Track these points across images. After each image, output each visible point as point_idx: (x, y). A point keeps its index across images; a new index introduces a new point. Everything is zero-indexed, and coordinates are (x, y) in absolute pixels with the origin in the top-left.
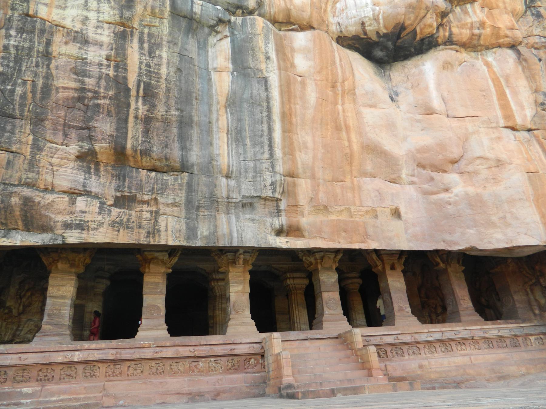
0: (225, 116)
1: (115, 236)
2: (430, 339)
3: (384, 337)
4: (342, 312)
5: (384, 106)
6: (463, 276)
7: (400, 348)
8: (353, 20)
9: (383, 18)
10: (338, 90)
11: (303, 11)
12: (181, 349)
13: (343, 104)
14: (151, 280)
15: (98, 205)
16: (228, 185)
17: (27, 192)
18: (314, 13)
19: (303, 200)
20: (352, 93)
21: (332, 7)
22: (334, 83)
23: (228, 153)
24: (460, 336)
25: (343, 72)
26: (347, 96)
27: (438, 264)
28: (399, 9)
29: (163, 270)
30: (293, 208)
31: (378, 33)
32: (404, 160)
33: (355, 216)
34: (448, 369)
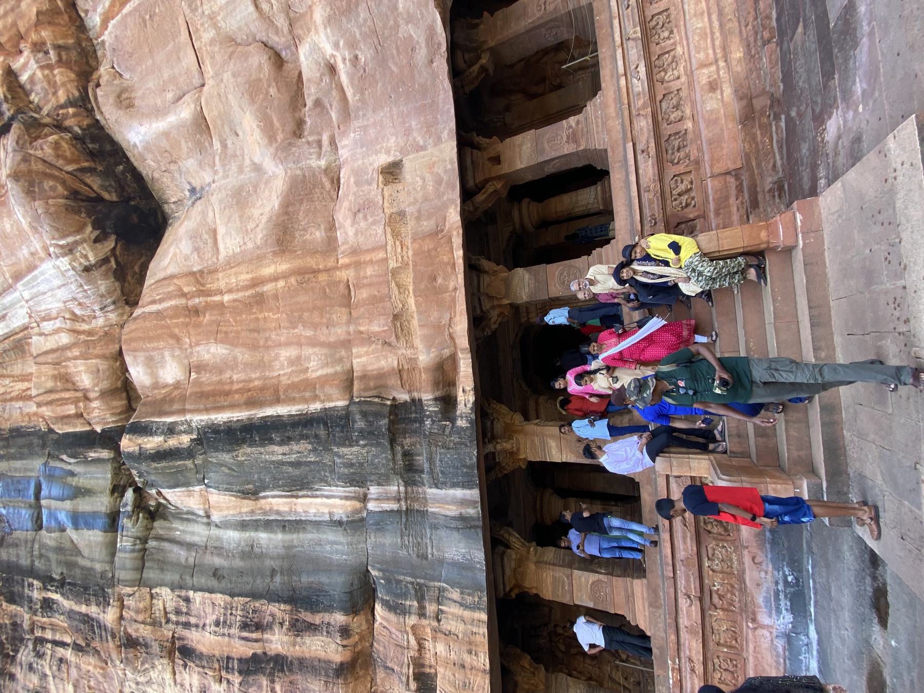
0: (270, 500)
2: (642, 69)
3: (644, 182)
4: (585, 258)
5: (211, 214)
7: (667, 140)
8: (86, 288)
9: (63, 237)
10: (200, 302)
11: (98, 371)
12: (684, 621)
13: (221, 293)
14: (550, 589)
16: (376, 499)
18: (96, 352)
20: (201, 276)
21: (84, 321)
22: (189, 311)
23: (328, 497)
25: (169, 297)
27: (483, 69)
28: (40, 211)
29: (532, 567)
30: (405, 377)
31: (96, 241)
32: (291, 165)
33: (405, 258)
34: (714, 17)
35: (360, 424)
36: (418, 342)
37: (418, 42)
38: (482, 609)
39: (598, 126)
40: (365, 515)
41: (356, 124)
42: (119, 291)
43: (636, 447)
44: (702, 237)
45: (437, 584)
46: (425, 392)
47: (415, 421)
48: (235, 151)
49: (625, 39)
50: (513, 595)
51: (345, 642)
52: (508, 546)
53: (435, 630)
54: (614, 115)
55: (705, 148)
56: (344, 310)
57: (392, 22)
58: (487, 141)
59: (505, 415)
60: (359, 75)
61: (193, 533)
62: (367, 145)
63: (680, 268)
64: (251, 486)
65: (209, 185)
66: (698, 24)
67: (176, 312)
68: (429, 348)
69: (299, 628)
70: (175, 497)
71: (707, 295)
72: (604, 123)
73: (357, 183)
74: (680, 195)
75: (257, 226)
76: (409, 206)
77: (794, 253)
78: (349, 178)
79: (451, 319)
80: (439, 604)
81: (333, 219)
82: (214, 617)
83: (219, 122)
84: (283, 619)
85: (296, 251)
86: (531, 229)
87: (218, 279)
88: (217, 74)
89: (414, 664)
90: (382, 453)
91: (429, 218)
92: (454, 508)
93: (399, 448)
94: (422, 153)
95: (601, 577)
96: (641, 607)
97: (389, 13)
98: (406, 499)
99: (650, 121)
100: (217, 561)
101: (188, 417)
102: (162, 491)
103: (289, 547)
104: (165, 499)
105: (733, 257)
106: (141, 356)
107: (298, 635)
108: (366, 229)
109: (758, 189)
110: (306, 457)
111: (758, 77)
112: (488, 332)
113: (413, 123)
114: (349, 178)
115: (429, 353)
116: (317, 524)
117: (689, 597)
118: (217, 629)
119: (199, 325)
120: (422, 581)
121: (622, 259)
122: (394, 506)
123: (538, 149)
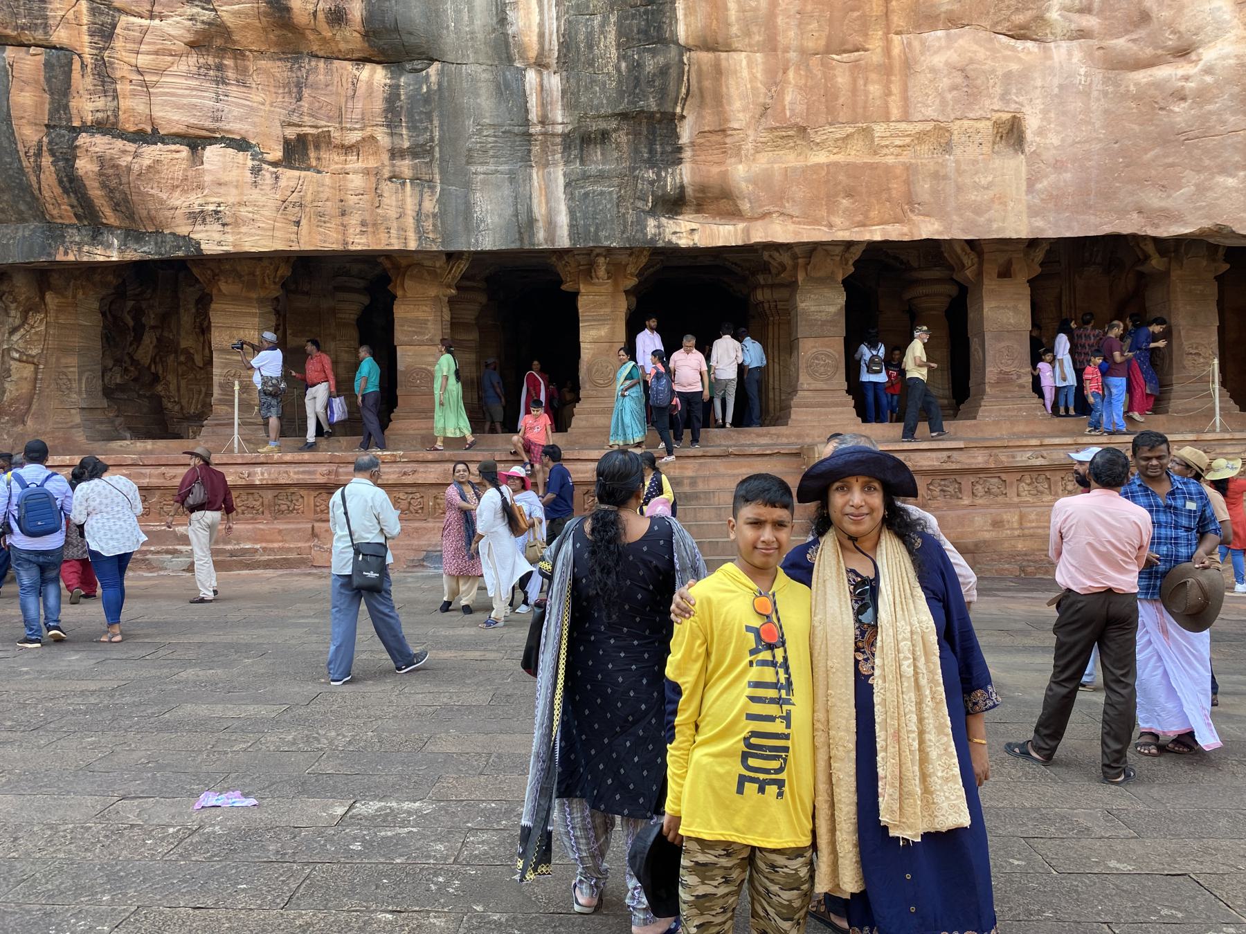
1: (293, 237)
3: (917, 454)
14: (409, 315)
15: (250, 163)
16: (542, 86)
17: (99, 143)
19: (739, 113)
27: (1147, 257)
29: (433, 292)
30: (714, 138)
33: (885, 151)
35: (651, 65)
37: (1169, 196)
41: (1098, 76)
45: (437, 177)
46: (692, 169)
47: (651, 151)
51: (321, 16)
54: (1015, 430)
56: (823, 42)
57: (1207, 162)
60: (1159, 99)
68: (754, 181)
73: (1008, 76)
76: (957, 162)
79: (792, 217)
89: (318, 136)
90: (608, 99)
91: (935, 192)
92: (543, 211)
94: (1024, 188)
97: (1219, 161)
98: (544, 134)
108: (936, 89)
113: (1068, 176)
114: (1020, 59)
115: (748, 180)
120: (437, 155)
122: (534, 116)
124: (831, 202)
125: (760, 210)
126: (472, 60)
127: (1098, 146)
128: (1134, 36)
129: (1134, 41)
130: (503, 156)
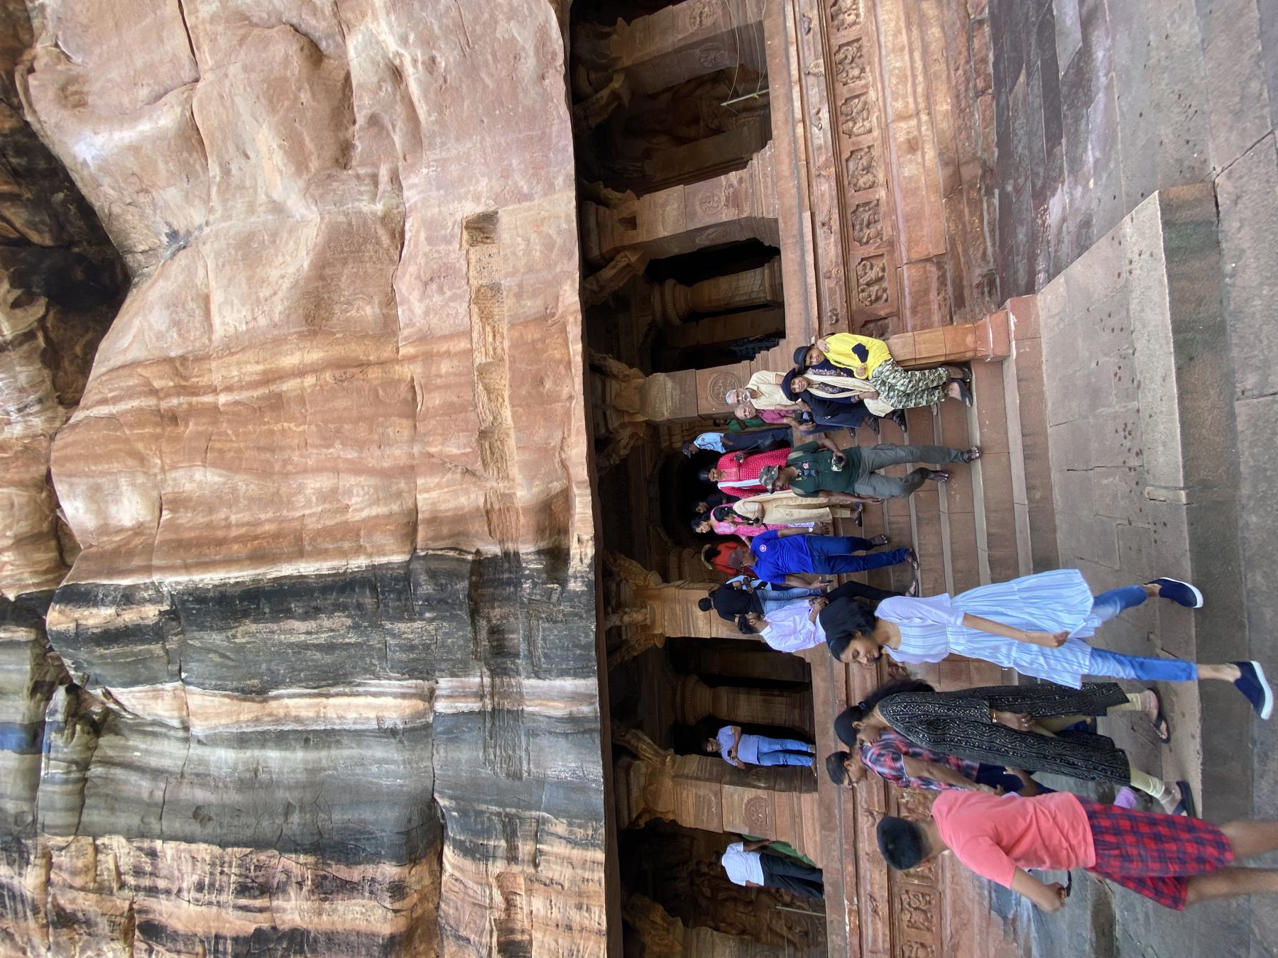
0: (286, 701)
2: (825, 115)
3: (821, 265)
5: (201, 272)
6: (640, 19)
7: (854, 212)
10: (180, 404)
13: (215, 391)
14: (692, 811)
16: (449, 697)
19: (470, 498)
20: (182, 365)
22: (162, 417)
23: (375, 695)
24: (814, 14)
25: (129, 394)
26: (195, 380)
27: (615, 96)
29: (668, 783)
33: (499, 351)
34: (917, 55)
35: (426, 588)
36: (515, 472)
37: (523, 48)
38: (598, 846)
39: (766, 187)
40: (431, 719)
41: (430, 155)
42: (48, 383)
43: (807, 615)
44: (894, 340)
45: (534, 813)
46: (524, 542)
48: (242, 181)
49: (803, 73)
50: (642, 823)
51: (397, 906)
52: (635, 756)
53: (530, 880)
54: (787, 174)
55: (901, 226)
56: (405, 422)
57: (486, 16)
58: (619, 195)
59: (636, 575)
60: (437, 85)
61: (161, 754)
62: (447, 186)
63: (867, 379)
64: (256, 682)
65: (200, 228)
66: (896, 63)
67: (140, 417)
68: (531, 479)
69: (326, 889)
70: (132, 699)
71: (899, 416)
72: (775, 184)
73: (430, 240)
74: (869, 284)
75: (275, 293)
77: (1005, 365)
78: (418, 232)
79: (563, 438)
80: (537, 841)
81: (393, 290)
82: (195, 878)
83: (218, 135)
84: (302, 876)
85: (334, 334)
86: (677, 322)
87: (210, 370)
88: (218, 66)
89: (500, 930)
90: (458, 630)
91: (535, 294)
92: (561, 705)
93: (483, 623)
94: (526, 204)
95: (760, 792)
96: (811, 831)
99: (833, 184)
100: (201, 795)
101: (156, 578)
102: (113, 690)
103: (313, 771)
104: (117, 702)
105: (933, 367)
106: (82, 484)
107: (325, 900)
108: (442, 307)
109: (965, 283)
110: (343, 636)
111: (969, 138)
112: (615, 460)
114: (418, 232)
115: (530, 486)
116: (358, 736)
117: (872, 814)
118: (199, 896)
119: (177, 439)
120: (513, 811)
121: (794, 365)
122: (475, 705)
123: (688, 213)
124: (546, 400)
125: (559, 471)
126: (429, 764)
127: (488, 139)
128: (390, 127)
129: (394, 126)
130: (513, 740)
